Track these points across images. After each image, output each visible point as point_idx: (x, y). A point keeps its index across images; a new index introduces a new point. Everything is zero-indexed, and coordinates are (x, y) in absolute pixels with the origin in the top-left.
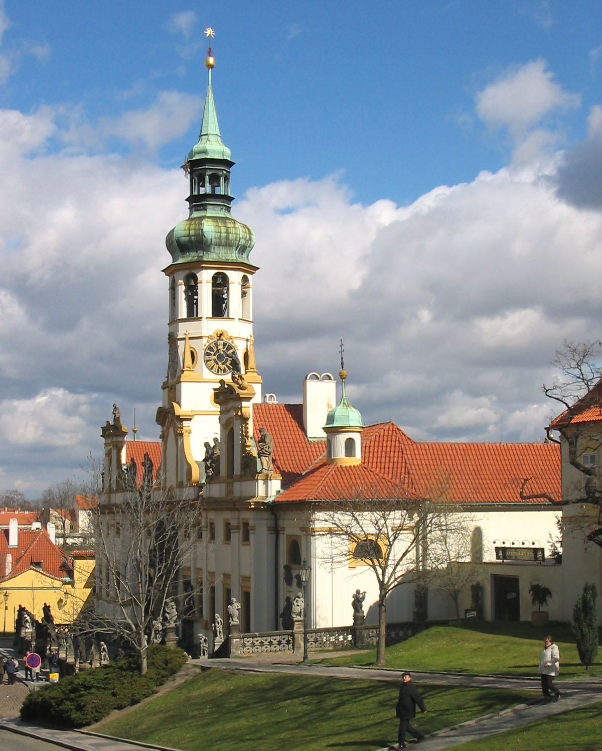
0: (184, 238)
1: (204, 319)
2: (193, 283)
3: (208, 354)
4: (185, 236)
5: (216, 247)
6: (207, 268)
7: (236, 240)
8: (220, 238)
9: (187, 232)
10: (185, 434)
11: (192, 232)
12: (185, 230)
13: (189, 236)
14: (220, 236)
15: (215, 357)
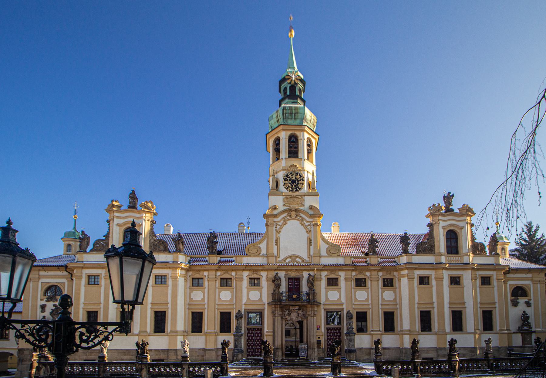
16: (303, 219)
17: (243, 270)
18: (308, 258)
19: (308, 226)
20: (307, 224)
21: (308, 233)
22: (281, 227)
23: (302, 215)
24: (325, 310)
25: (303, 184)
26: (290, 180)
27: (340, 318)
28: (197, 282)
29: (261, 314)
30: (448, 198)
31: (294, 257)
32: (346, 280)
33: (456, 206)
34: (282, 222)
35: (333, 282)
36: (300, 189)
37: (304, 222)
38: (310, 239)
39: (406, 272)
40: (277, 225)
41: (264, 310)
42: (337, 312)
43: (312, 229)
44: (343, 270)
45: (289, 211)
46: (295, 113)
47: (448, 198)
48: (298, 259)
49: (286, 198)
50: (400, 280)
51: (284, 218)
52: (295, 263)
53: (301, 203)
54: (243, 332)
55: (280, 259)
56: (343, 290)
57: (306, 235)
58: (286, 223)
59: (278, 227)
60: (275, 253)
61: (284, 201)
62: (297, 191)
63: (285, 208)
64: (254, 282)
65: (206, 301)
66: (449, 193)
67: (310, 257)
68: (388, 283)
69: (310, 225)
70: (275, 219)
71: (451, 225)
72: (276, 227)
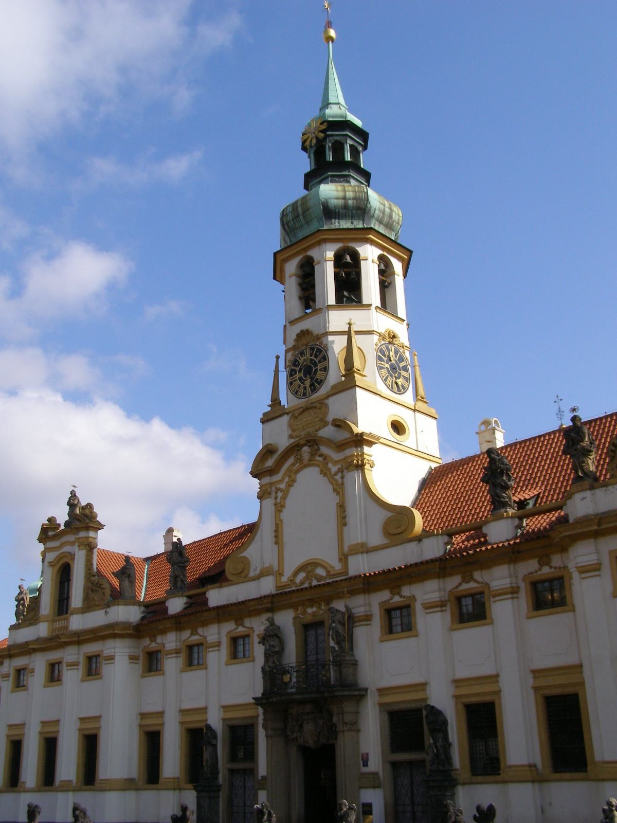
0: (336, 201)
1: (373, 307)
2: (348, 259)
3: (379, 358)
4: (338, 198)
5: (377, 223)
6: (373, 243)
7: (398, 223)
8: (383, 212)
9: (341, 194)
10: (367, 467)
11: (350, 194)
12: (337, 191)
13: (344, 198)
14: (384, 210)
15: (388, 366)
19: (336, 474)
20: (334, 469)
21: (338, 493)
22: (286, 494)
23: (324, 450)
24: (381, 705)
25: (326, 369)
26: (300, 371)
28: (152, 663)
31: (308, 567)
34: (287, 479)
35: (398, 621)
36: (320, 382)
37: (330, 465)
38: (342, 507)
40: (278, 490)
43: (345, 480)
46: (304, 213)
48: (320, 572)
49: (294, 417)
51: (289, 470)
52: (315, 583)
53: (322, 420)
54: (221, 780)
55: (284, 579)
57: (335, 499)
58: (294, 481)
59: (280, 494)
60: (276, 568)
61: (290, 426)
62: (314, 389)
63: (292, 441)
64: (237, 648)
67: (344, 558)
68: (548, 596)
69: (341, 471)
72: (276, 498)
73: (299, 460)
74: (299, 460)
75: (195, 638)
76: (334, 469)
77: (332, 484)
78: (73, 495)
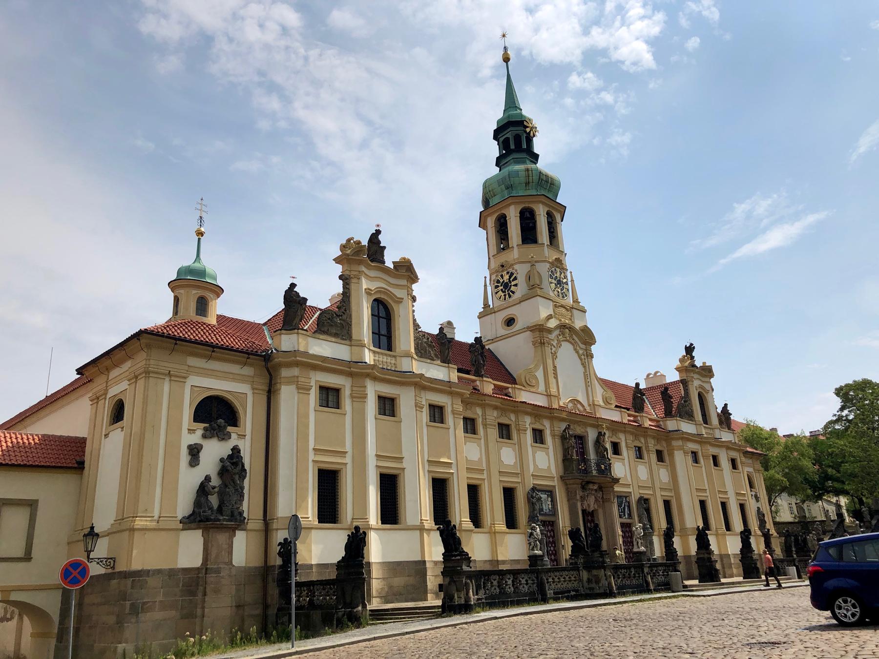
16: (576, 342)
17: (527, 413)
18: (590, 405)
27: (629, 507)
29: (551, 493)
30: (690, 349)
31: (575, 401)
32: (627, 447)
33: (698, 363)
39: (680, 443)
41: (554, 487)
42: (626, 497)
44: (625, 432)
45: (562, 327)
47: (690, 349)
50: (671, 455)
56: (626, 461)
59: (554, 349)
64: (538, 436)
65: (484, 466)
66: (692, 344)
70: (550, 336)
71: (701, 387)
73: (563, 334)
74: (563, 334)
75: (505, 421)
76: (581, 352)
77: (581, 359)
78: (378, 232)
